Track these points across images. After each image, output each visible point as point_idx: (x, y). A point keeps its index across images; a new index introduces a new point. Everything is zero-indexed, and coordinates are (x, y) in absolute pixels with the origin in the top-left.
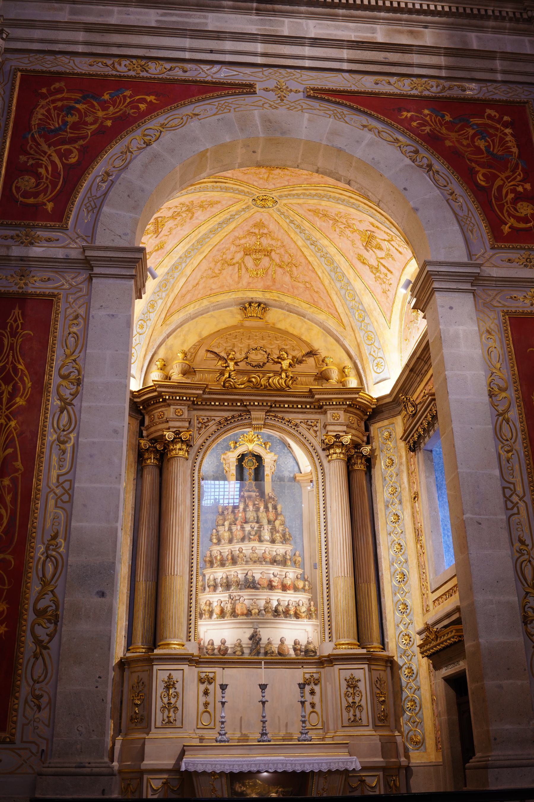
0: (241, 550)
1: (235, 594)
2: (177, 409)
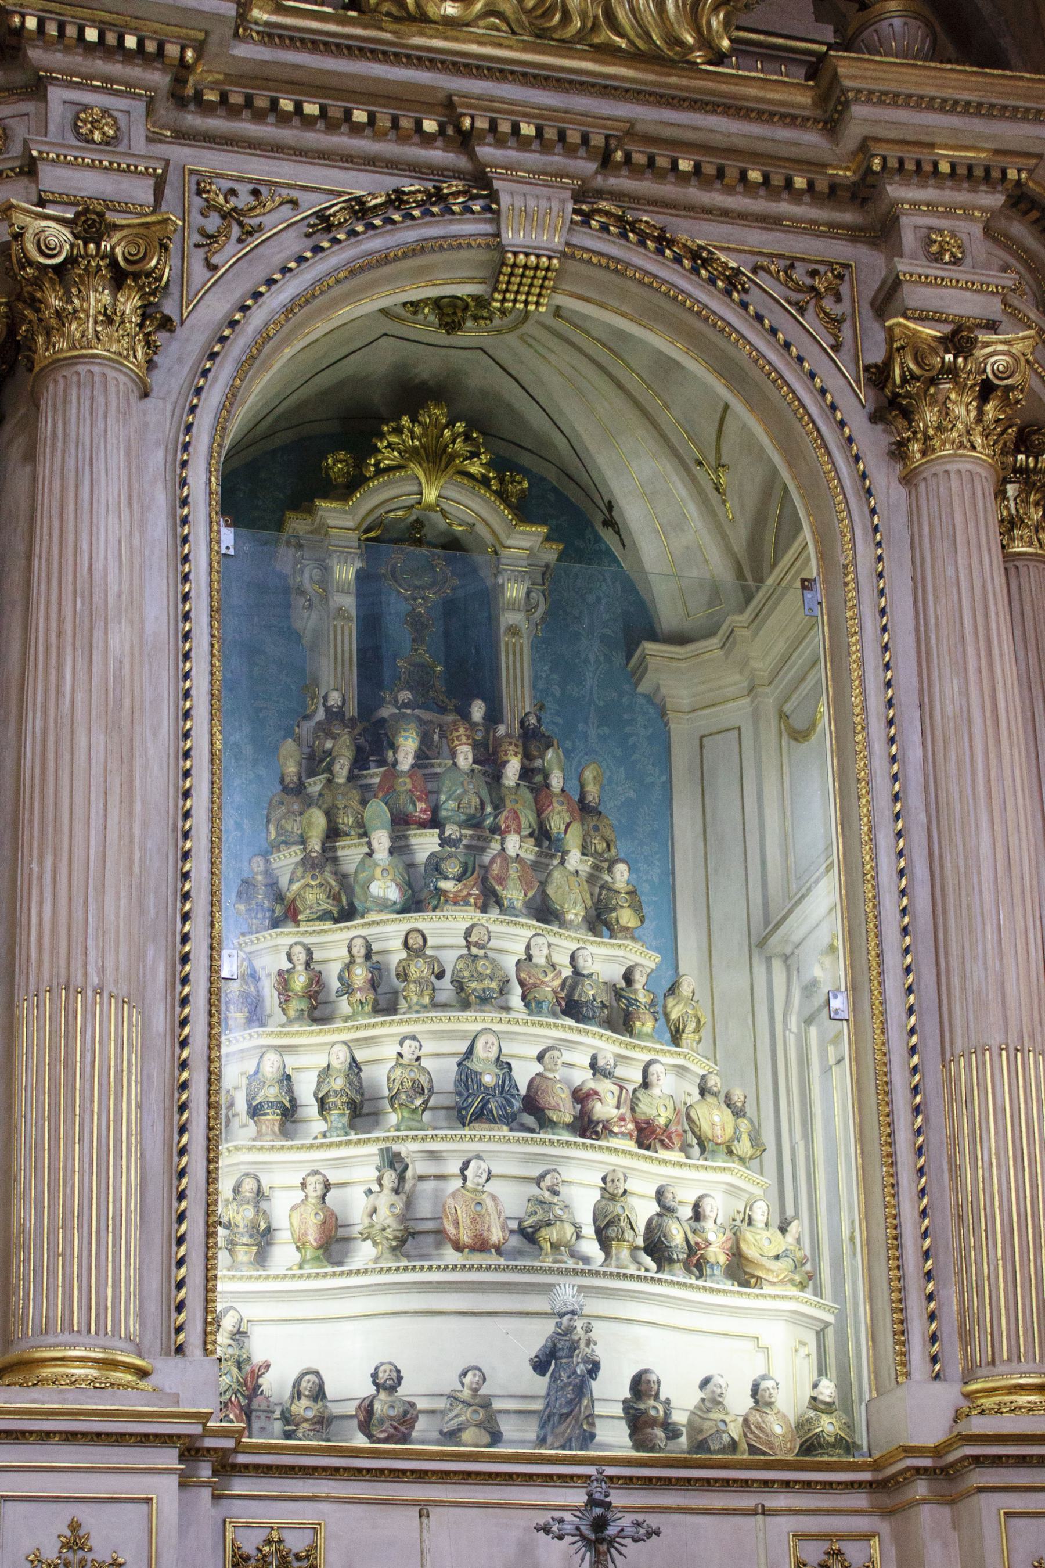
0: (415, 941)
2: (86, 108)
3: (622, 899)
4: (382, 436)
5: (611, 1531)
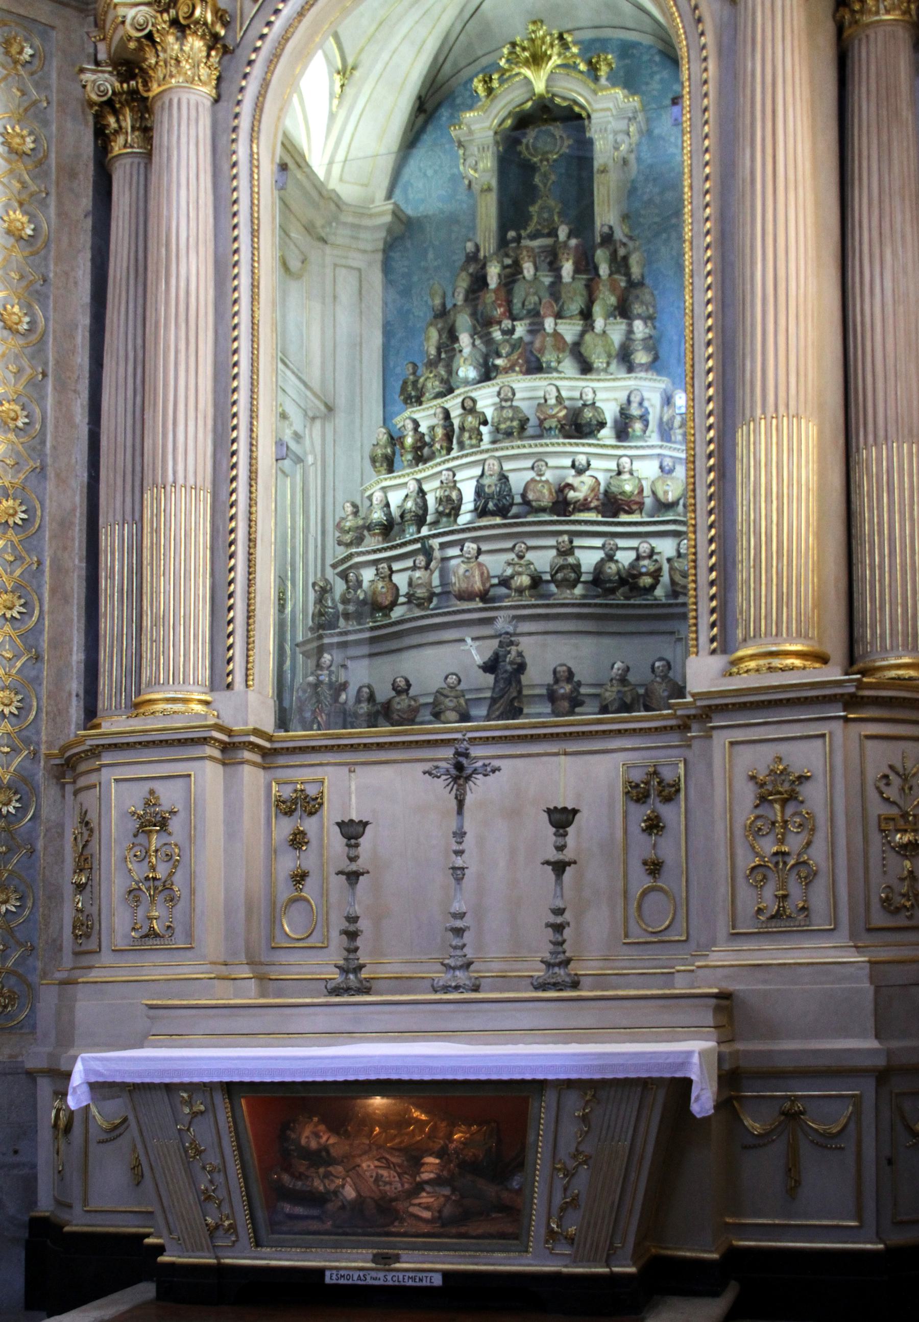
0: (469, 404)
3: (638, 346)
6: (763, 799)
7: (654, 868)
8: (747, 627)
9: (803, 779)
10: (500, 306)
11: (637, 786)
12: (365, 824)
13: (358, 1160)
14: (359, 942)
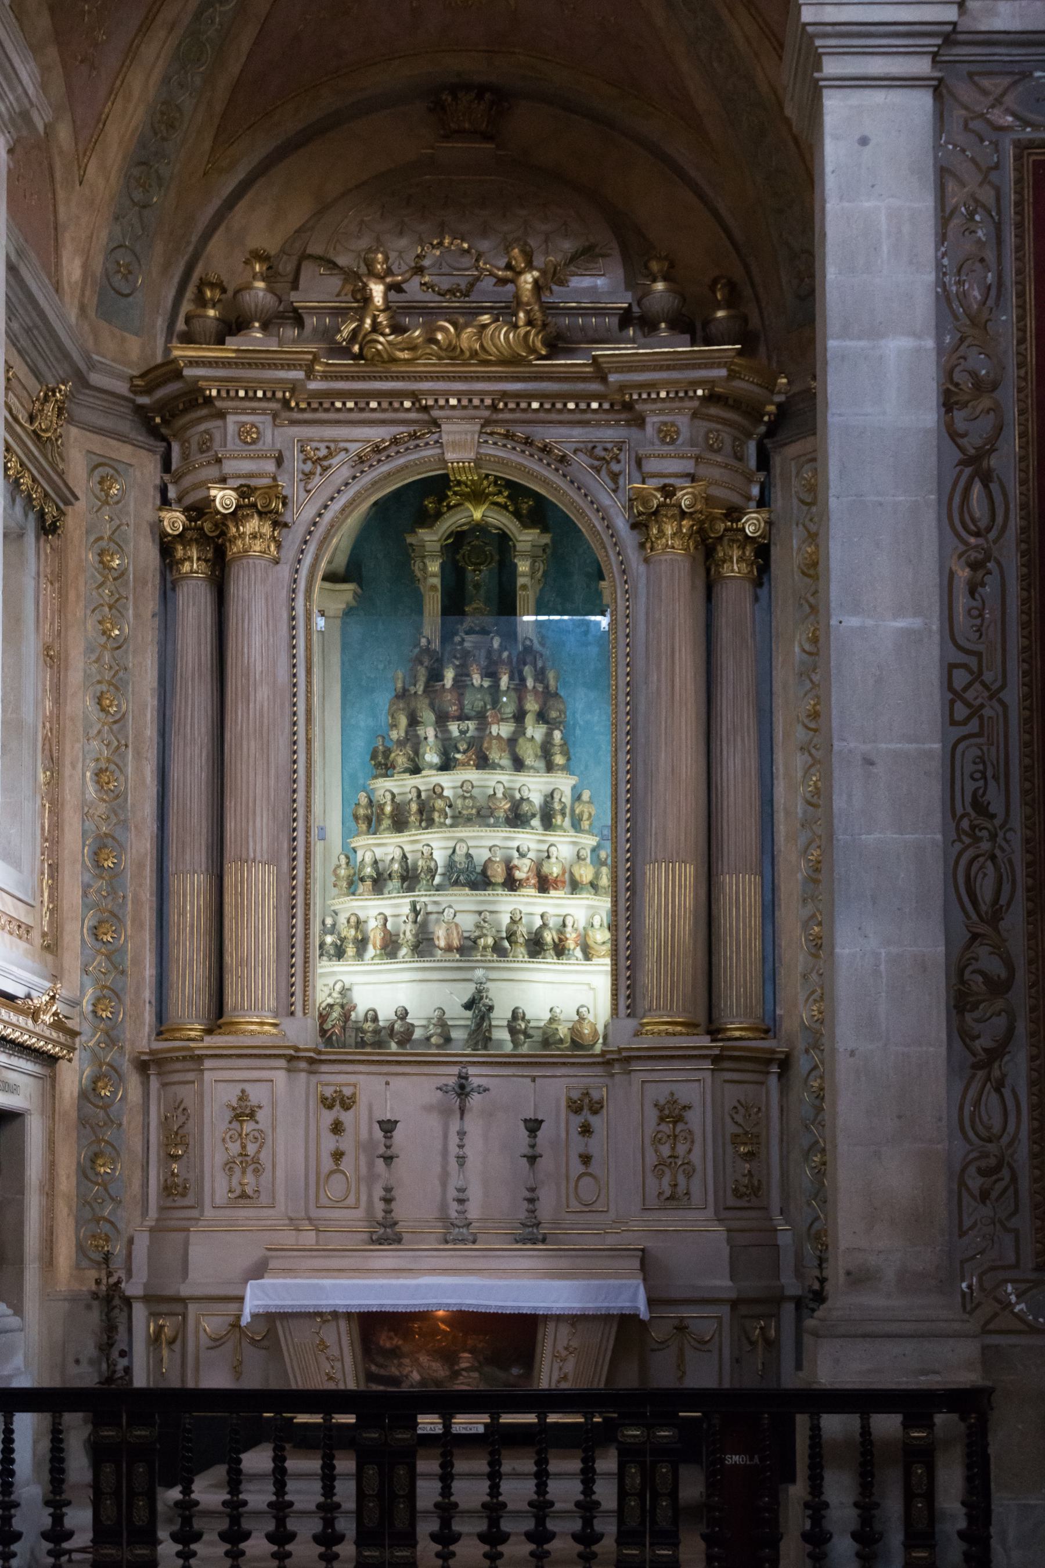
1: (423, 899)
2: (244, 424)
4: (450, 488)
5: (468, 1089)
6: (662, 1119)
7: (586, 1159)
8: (651, 1002)
9: (686, 1108)
10: (454, 704)
11: (575, 1102)
12: (396, 1122)
13: (417, 1355)
14: (393, 1205)
